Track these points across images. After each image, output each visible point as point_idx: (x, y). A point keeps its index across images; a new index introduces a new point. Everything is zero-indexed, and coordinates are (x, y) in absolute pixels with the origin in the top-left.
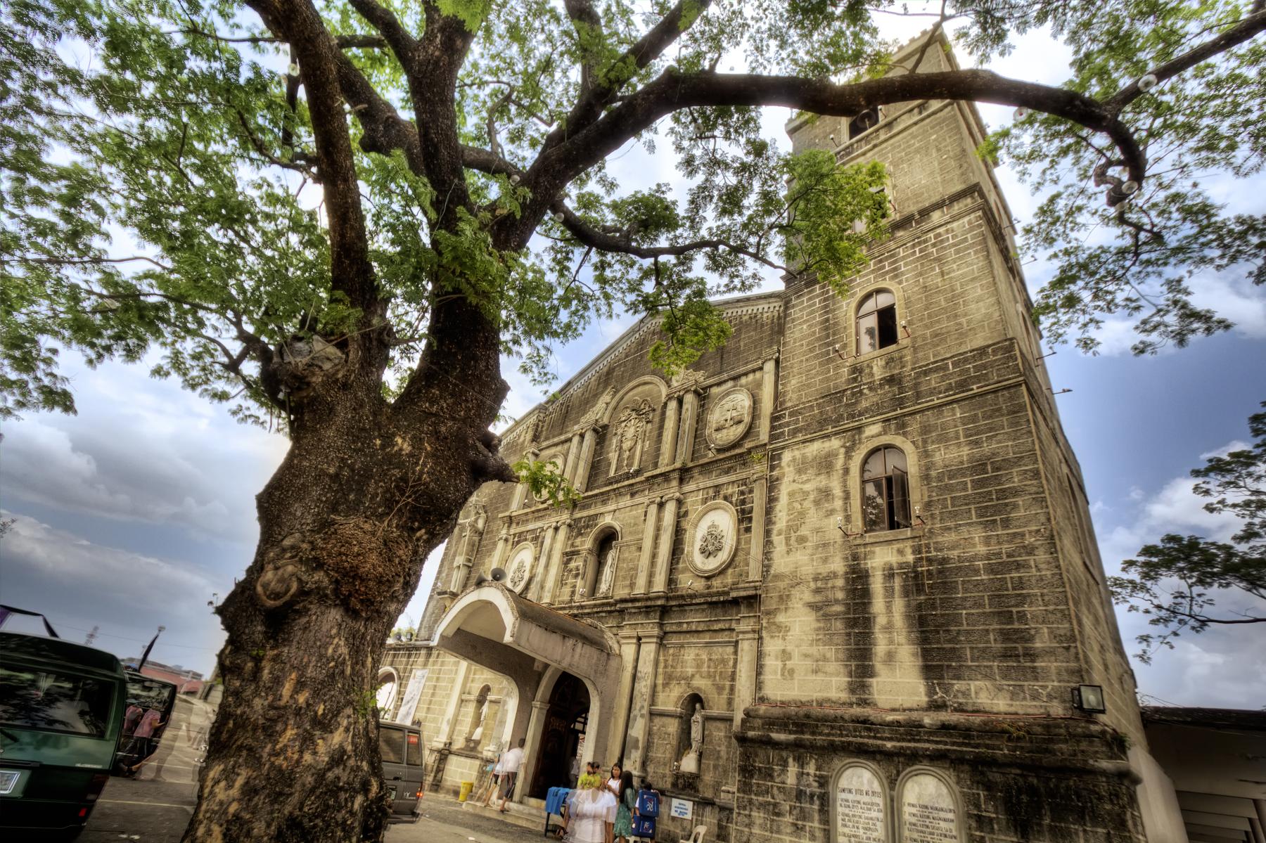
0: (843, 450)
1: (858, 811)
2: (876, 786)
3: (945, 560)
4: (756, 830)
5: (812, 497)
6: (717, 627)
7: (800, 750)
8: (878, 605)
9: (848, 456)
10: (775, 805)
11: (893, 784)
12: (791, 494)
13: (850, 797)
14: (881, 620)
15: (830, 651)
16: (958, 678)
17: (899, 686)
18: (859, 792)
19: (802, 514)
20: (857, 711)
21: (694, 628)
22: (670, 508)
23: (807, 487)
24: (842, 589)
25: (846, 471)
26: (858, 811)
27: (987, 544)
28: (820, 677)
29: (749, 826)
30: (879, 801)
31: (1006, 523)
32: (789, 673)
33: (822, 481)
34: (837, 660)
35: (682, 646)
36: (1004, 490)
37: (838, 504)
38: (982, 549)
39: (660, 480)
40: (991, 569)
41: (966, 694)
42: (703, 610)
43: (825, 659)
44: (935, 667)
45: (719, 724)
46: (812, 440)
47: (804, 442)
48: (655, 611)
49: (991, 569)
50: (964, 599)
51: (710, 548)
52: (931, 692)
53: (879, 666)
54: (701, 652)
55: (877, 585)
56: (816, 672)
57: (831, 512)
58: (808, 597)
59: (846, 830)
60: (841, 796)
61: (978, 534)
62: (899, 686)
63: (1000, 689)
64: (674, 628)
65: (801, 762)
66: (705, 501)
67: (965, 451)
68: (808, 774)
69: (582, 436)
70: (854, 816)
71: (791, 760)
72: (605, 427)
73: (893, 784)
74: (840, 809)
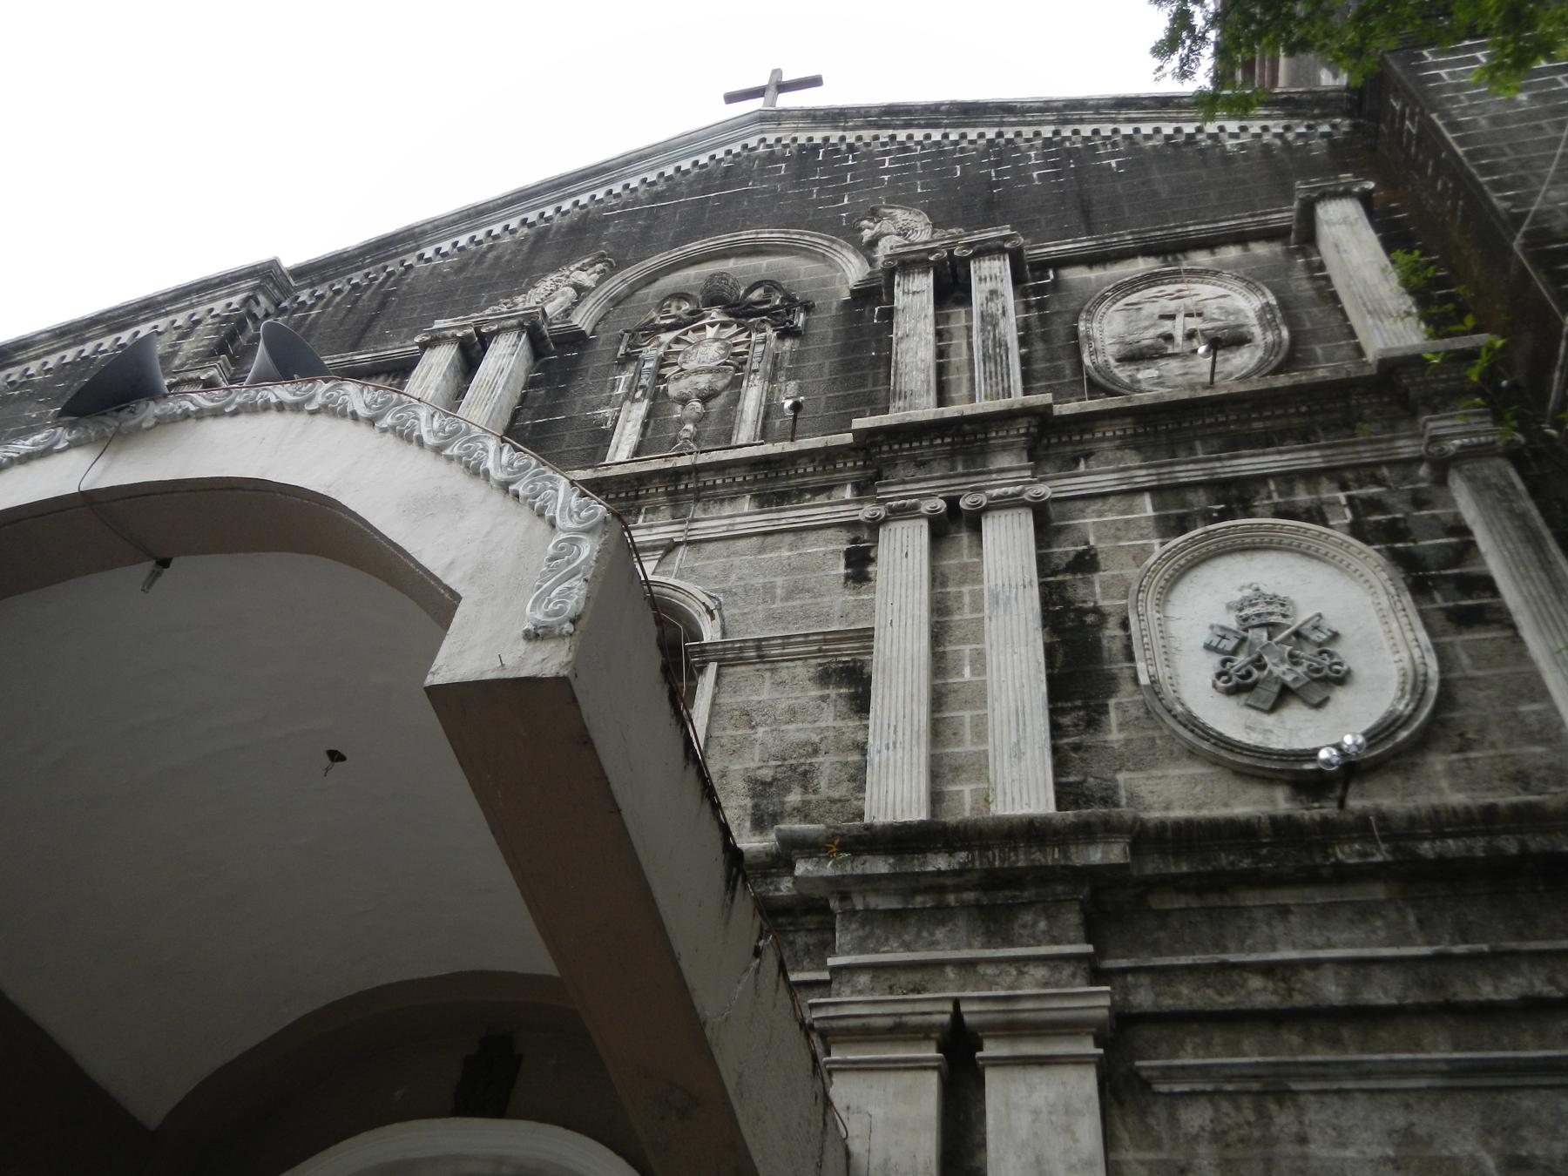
6: (1487, 991)
21: (1332, 991)
22: (1007, 547)
35: (1274, 1088)
39: (922, 448)
42: (1364, 912)
48: (1050, 908)
51: (1280, 669)
54: (1425, 1122)
64: (1187, 996)
66: (1172, 525)
69: (471, 355)
72: (577, 339)
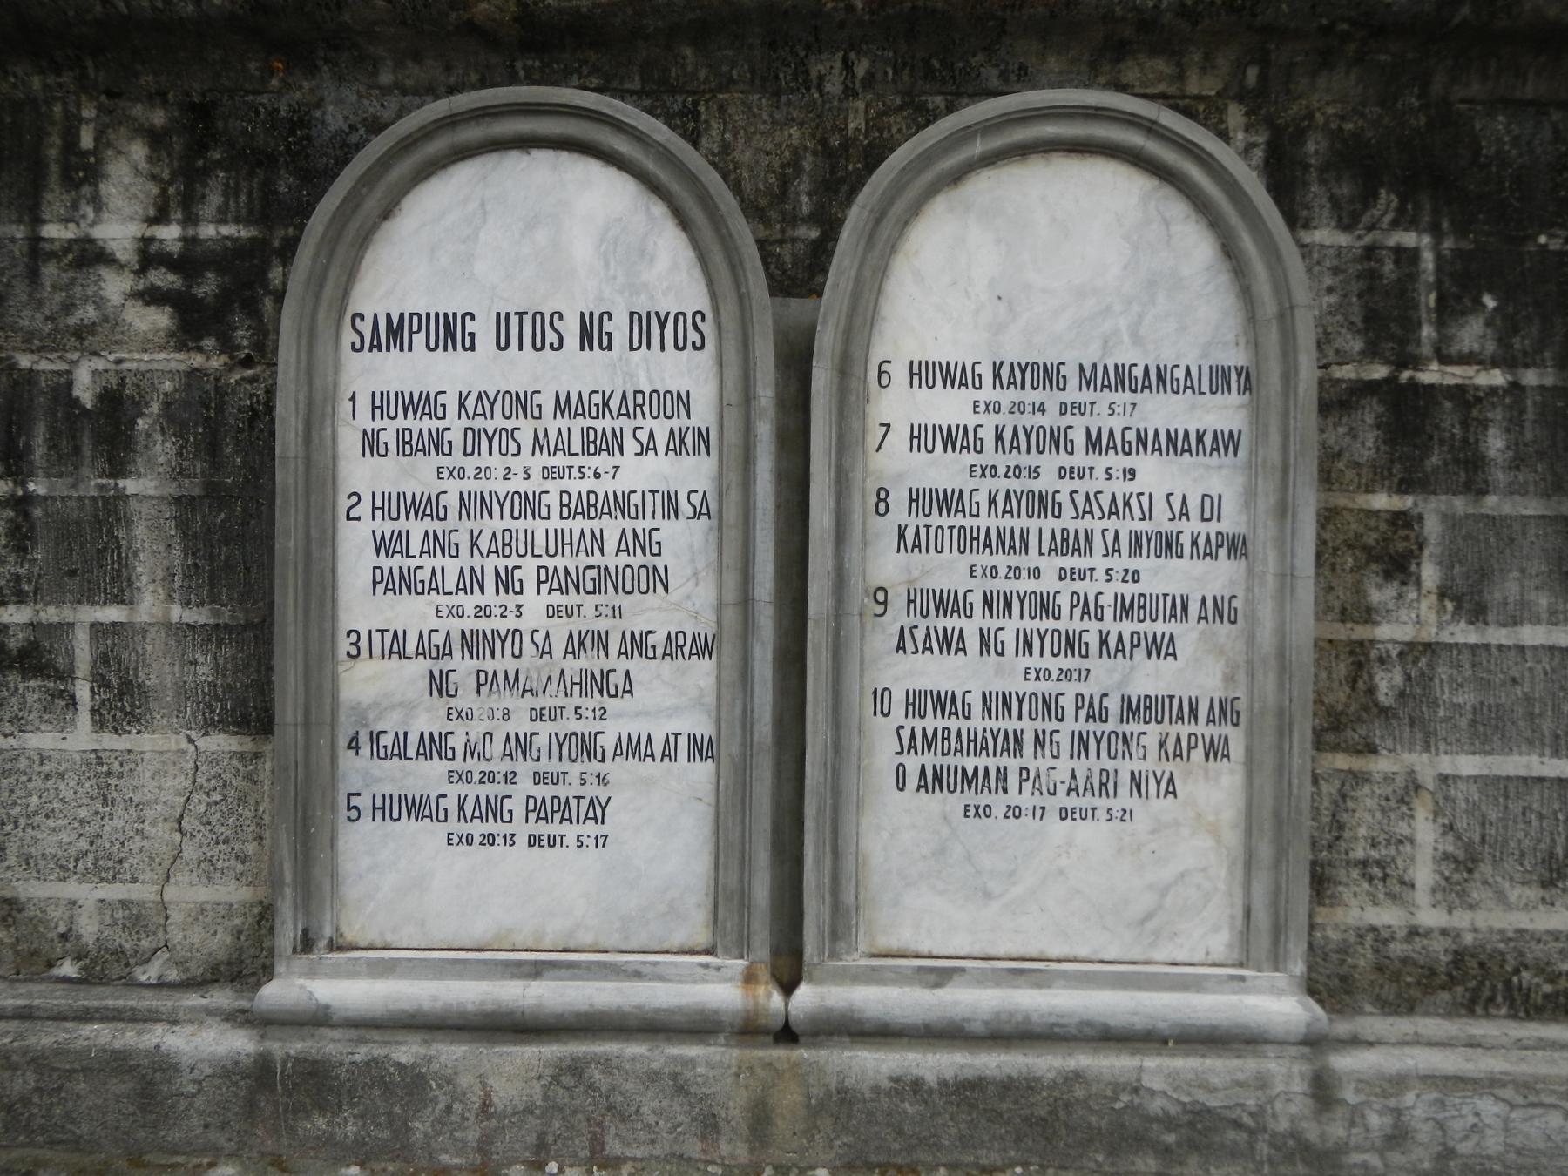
1: (519, 471)
2: (670, 273)
11: (794, 255)
18: (533, 329)
26: (519, 471)
30: (690, 374)
59: (413, 614)
60: (370, 374)
68: (90, 255)
70: (474, 504)
73: (794, 255)
74: (361, 474)
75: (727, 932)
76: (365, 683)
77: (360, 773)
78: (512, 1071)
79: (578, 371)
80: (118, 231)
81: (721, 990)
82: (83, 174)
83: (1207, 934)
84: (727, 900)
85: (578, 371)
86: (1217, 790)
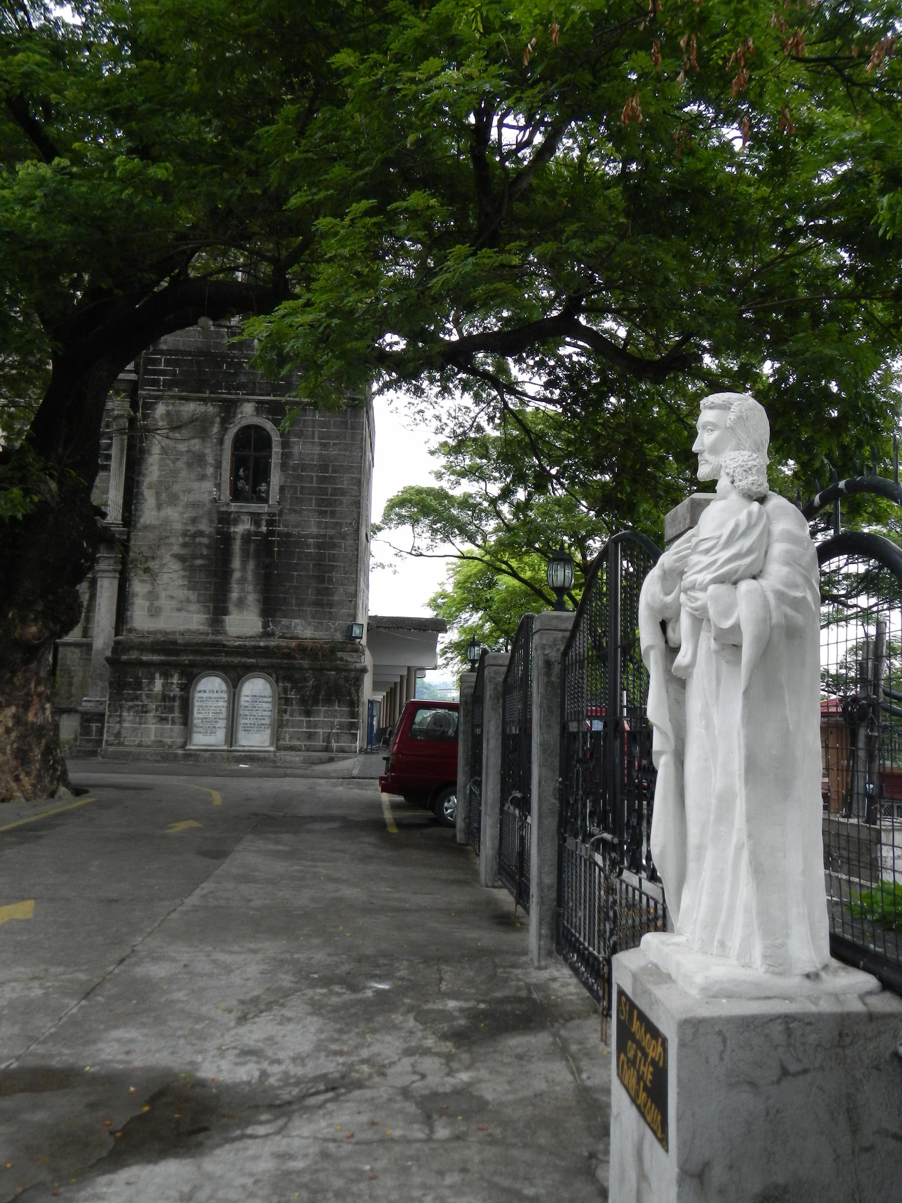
0: (218, 419)
2: (224, 687)
3: (288, 535)
4: (126, 725)
5: (185, 459)
7: (165, 669)
8: (236, 563)
9: (224, 430)
10: (143, 706)
11: (234, 685)
12: (164, 451)
13: (204, 695)
14: (237, 575)
15: (193, 596)
16: (285, 617)
17: (244, 623)
18: (212, 691)
19: (175, 473)
20: (210, 638)
23: (182, 447)
24: (208, 546)
25: (221, 442)
27: (319, 527)
28: (183, 614)
29: (120, 722)
30: (225, 696)
31: (333, 514)
32: (154, 612)
33: (196, 444)
34: (198, 602)
36: (336, 489)
37: (210, 471)
38: (314, 530)
40: (319, 546)
41: (288, 627)
43: (188, 601)
44: (270, 609)
45: (73, 648)
46: (187, 399)
47: (182, 398)
49: (319, 546)
50: (297, 564)
52: (266, 625)
53: (231, 607)
55: (237, 546)
56: (179, 610)
57: (203, 477)
58: (176, 549)
59: (201, 716)
60: (197, 695)
61: (314, 519)
62: (244, 623)
63: (309, 624)
65: (166, 675)
67: (317, 450)
71: (157, 676)
73: (234, 685)
74: (196, 704)
75: (226, 743)
76: (196, 722)
77: (195, 729)
78: (207, 754)
79: (216, 695)
80: (175, 681)
81: (225, 748)
82: (172, 676)
83: (267, 744)
84: (226, 740)
85: (216, 695)
86: (268, 732)
